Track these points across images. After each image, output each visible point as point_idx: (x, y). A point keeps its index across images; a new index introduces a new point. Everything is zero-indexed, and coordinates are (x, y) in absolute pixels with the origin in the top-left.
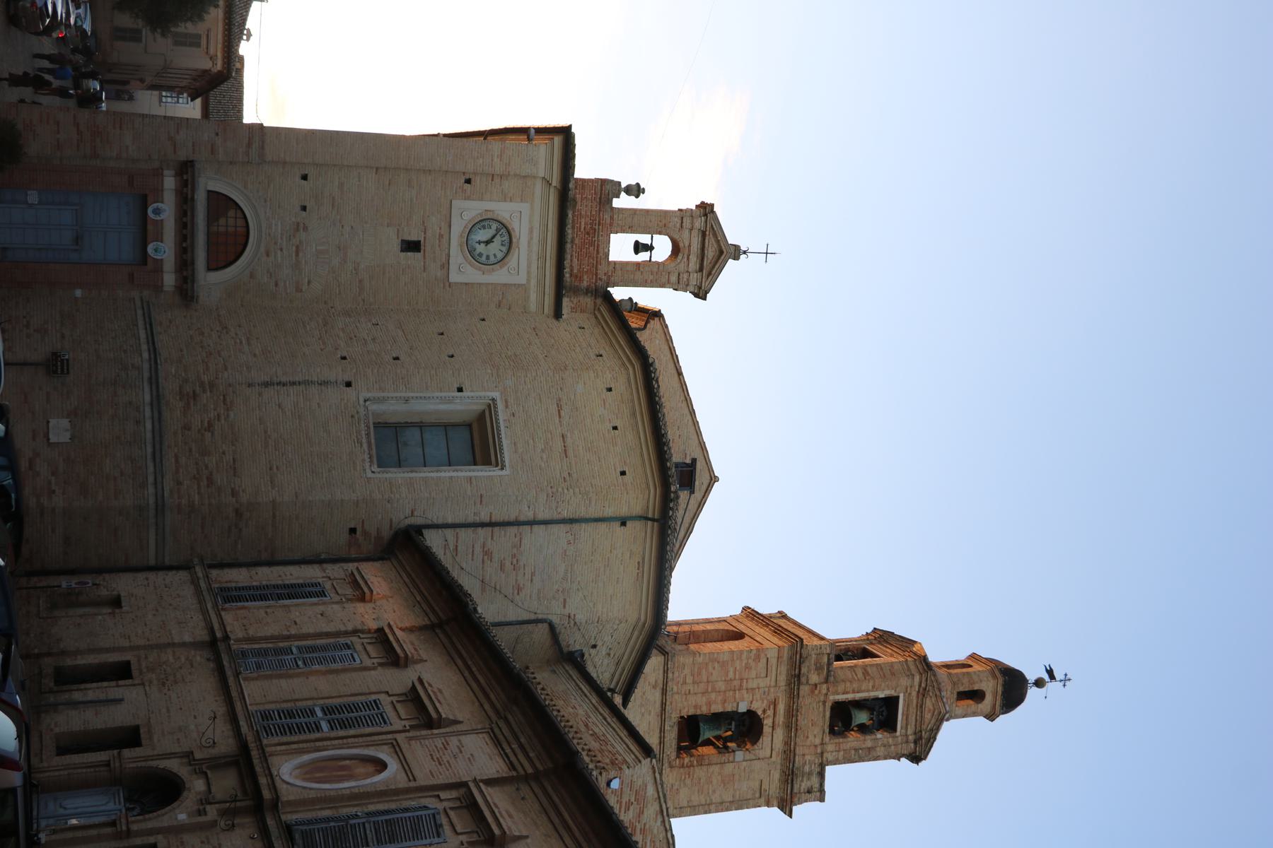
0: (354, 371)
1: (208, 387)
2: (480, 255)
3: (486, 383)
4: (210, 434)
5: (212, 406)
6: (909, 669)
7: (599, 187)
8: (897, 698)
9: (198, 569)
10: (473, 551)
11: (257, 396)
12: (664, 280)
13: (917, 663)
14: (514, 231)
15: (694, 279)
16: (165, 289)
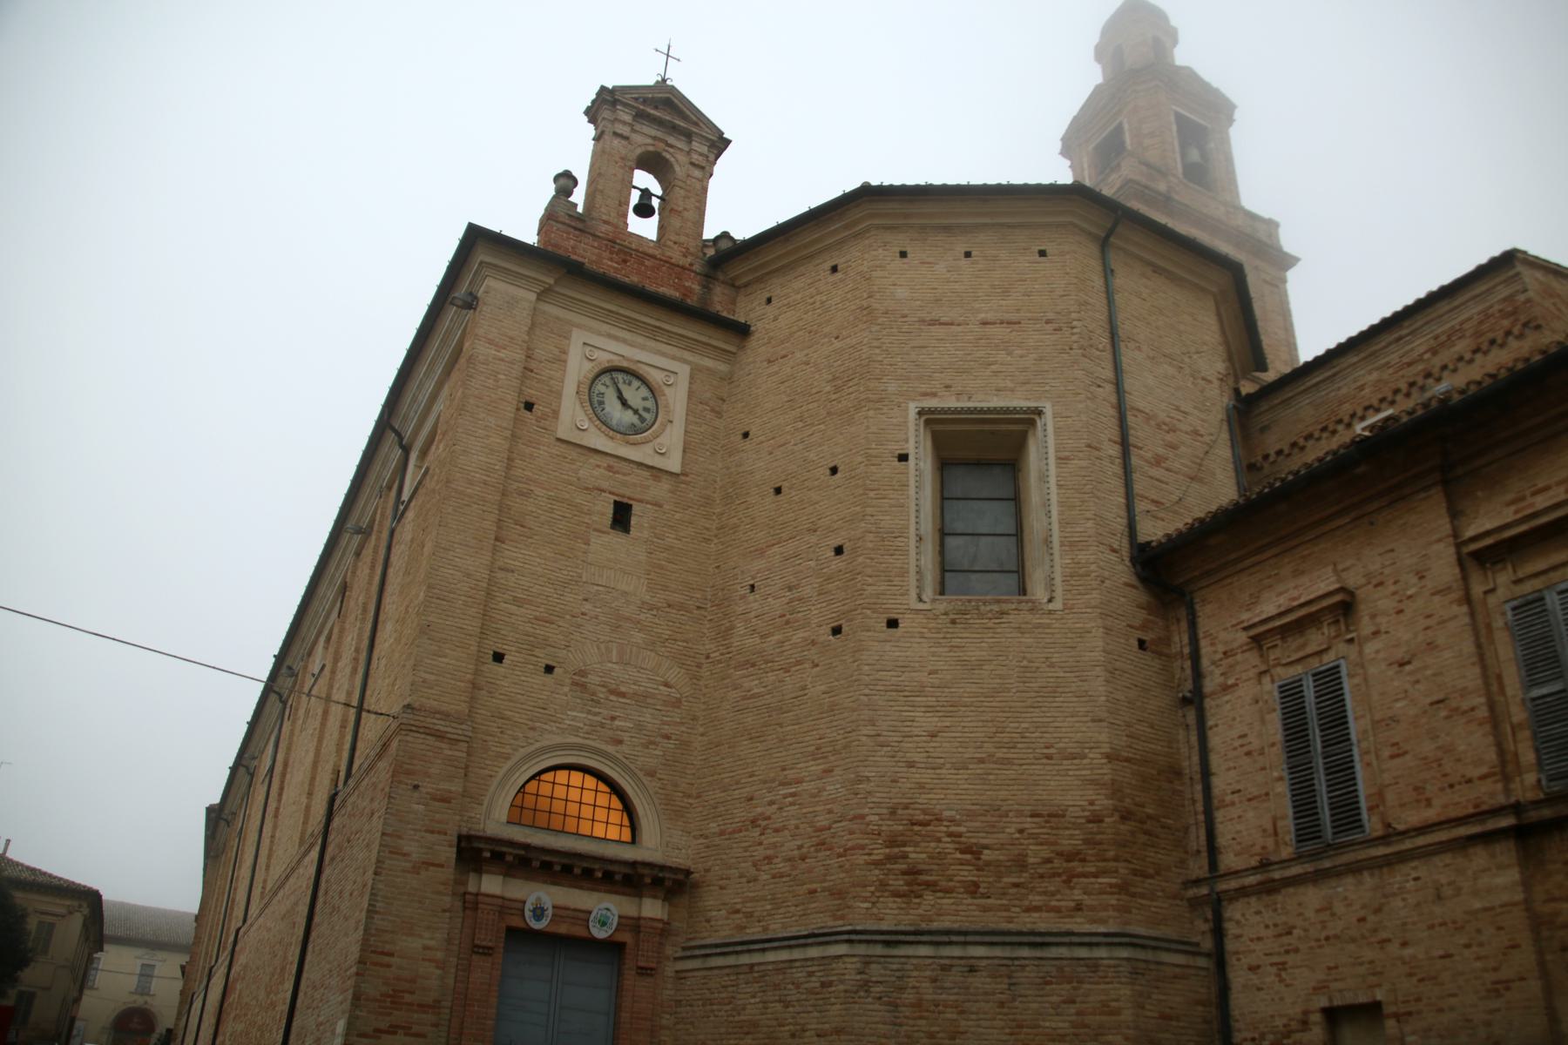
0: (869, 612)
1: (896, 850)
3: (894, 420)
4: (986, 852)
5: (933, 844)
7: (560, 226)
9: (1223, 886)
10: (1157, 480)
11: (914, 770)
12: (698, 185)
16: (665, 918)
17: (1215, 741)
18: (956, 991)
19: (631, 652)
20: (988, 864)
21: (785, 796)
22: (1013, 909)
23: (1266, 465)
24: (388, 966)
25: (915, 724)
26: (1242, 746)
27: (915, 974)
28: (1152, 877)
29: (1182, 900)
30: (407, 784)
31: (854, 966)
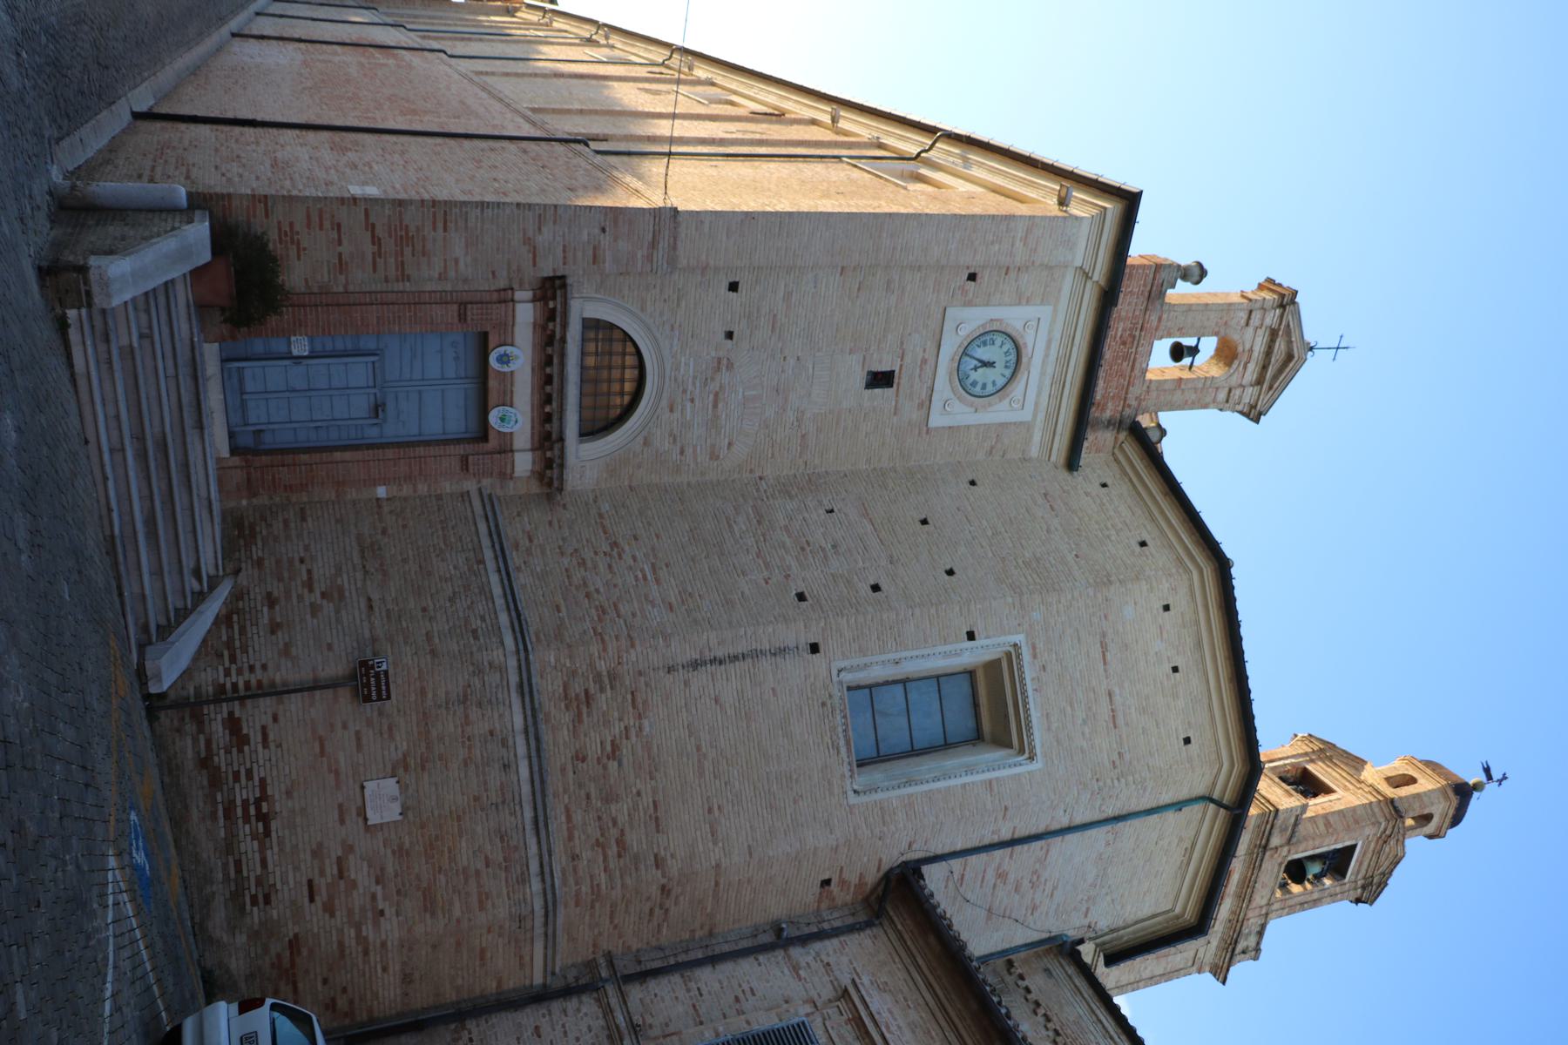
0: (822, 624)
2: (974, 384)
4: (616, 763)
5: (616, 714)
6: (1374, 814)
7: (1151, 276)
8: (1353, 847)
9: (611, 990)
10: (984, 877)
11: (682, 687)
12: (1208, 399)
13: (1382, 804)
14: (1026, 347)
15: (1249, 395)
16: (516, 474)
17: (746, 966)
18: (485, 755)
19: (755, 408)
20: (605, 768)
21: (642, 570)
22: (566, 797)
23: (1014, 977)
24: (435, 229)
25: (725, 682)
26: (743, 991)
27: (496, 716)
28: (611, 922)
29: (594, 953)
30: (605, 221)
31: (495, 657)
